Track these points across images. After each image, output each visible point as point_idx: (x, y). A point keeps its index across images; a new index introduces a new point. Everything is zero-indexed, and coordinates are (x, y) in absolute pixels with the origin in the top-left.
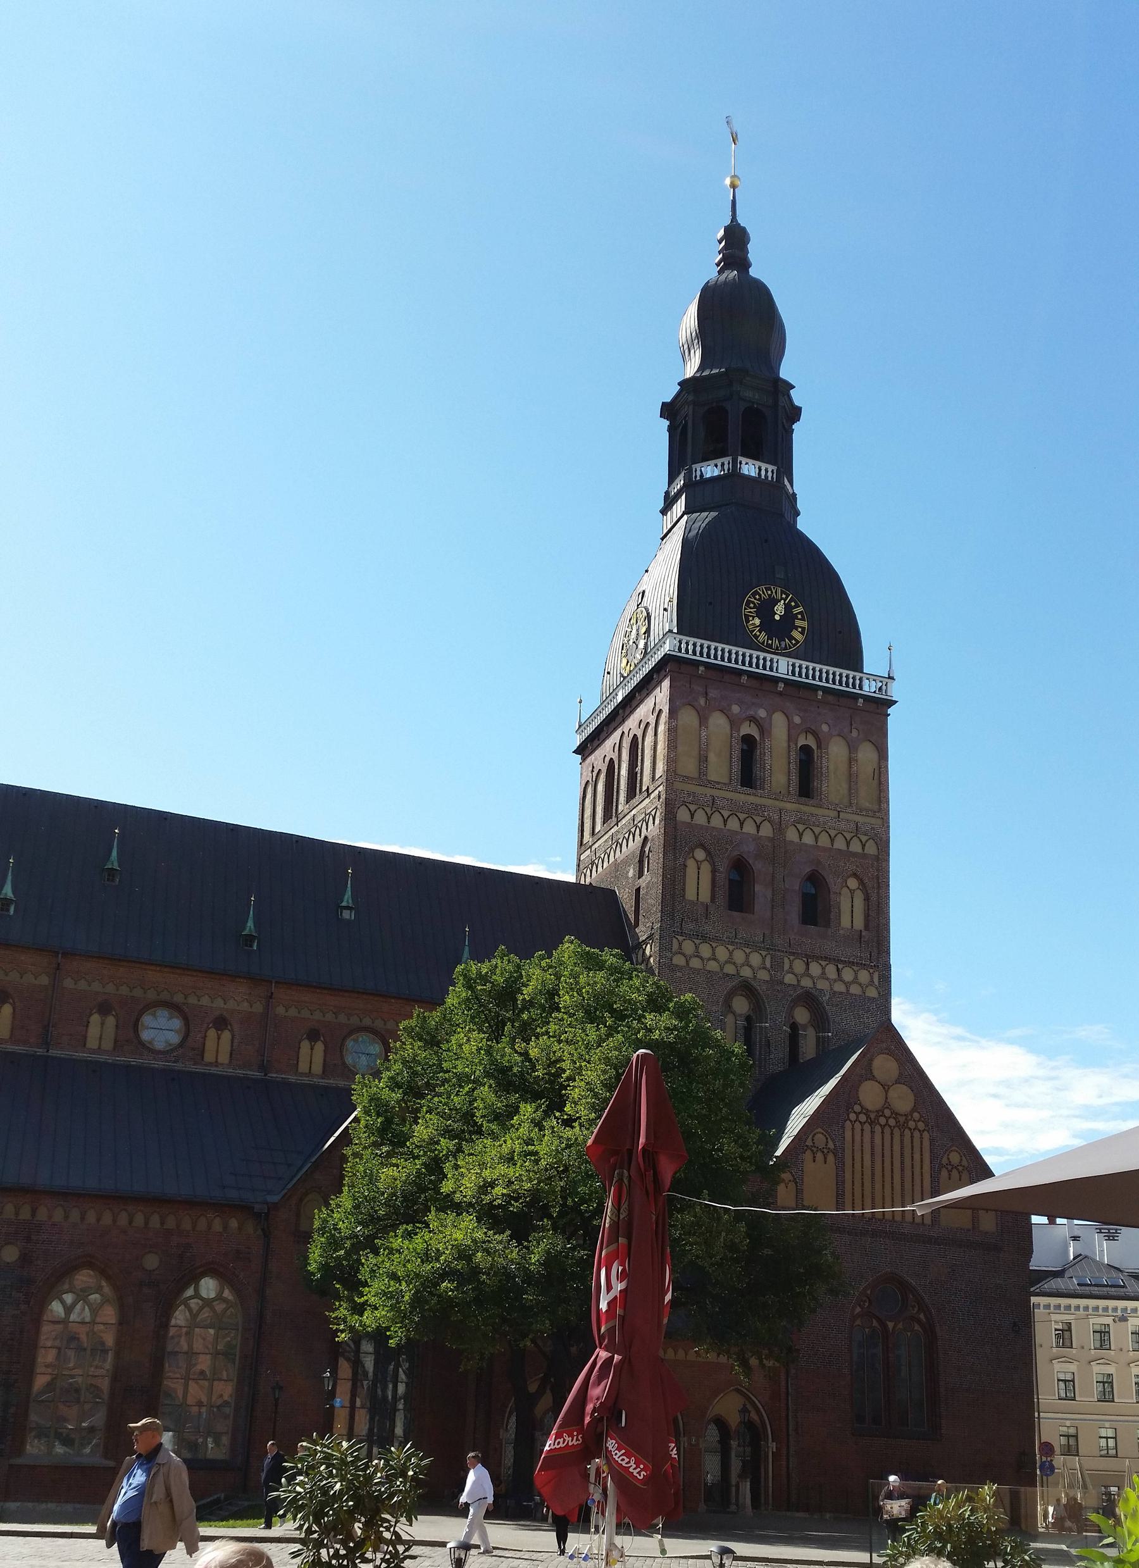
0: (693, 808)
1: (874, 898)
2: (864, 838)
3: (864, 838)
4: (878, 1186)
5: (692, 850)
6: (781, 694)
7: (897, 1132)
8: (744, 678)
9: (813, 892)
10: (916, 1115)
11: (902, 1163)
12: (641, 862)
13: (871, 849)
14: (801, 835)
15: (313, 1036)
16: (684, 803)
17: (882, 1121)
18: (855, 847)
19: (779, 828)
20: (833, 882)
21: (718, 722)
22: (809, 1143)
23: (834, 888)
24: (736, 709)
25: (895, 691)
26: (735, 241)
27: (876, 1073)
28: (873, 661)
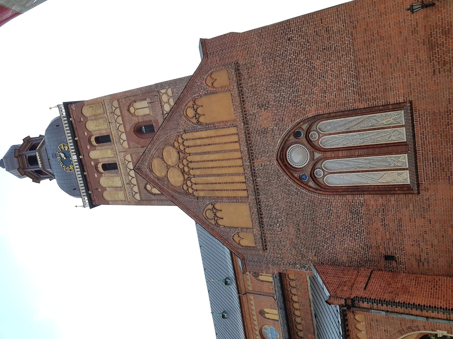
0: (134, 193)
1: (133, 99)
2: (114, 108)
3: (114, 108)
4: (224, 171)
5: (148, 191)
6: (84, 156)
7: (190, 158)
8: (85, 173)
9: (143, 128)
10: (176, 144)
11: (205, 153)
13: (116, 104)
14: (124, 141)
16: (133, 196)
17: (186, 169)
18: (118, 112)
19: (125, 151)
20: (135, 120)
22: (213, 222)
23: (137, 121)
24: (96, 175)
27: (163, 174)
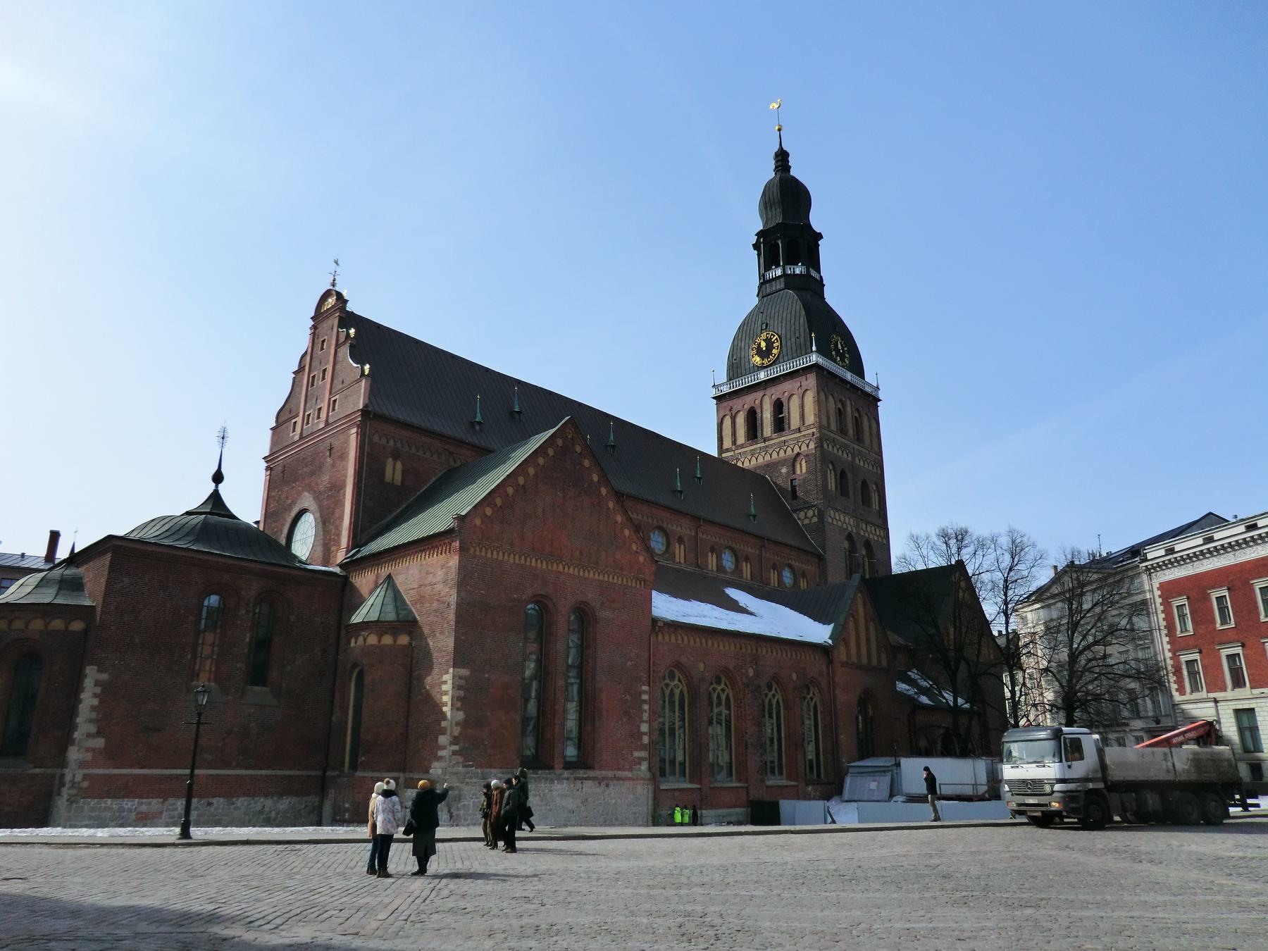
12: (794, 466)
15: (713, 550)
21: (831, 399)
25: (881, 395)
26: (782, 158)
28: (870, 377)
